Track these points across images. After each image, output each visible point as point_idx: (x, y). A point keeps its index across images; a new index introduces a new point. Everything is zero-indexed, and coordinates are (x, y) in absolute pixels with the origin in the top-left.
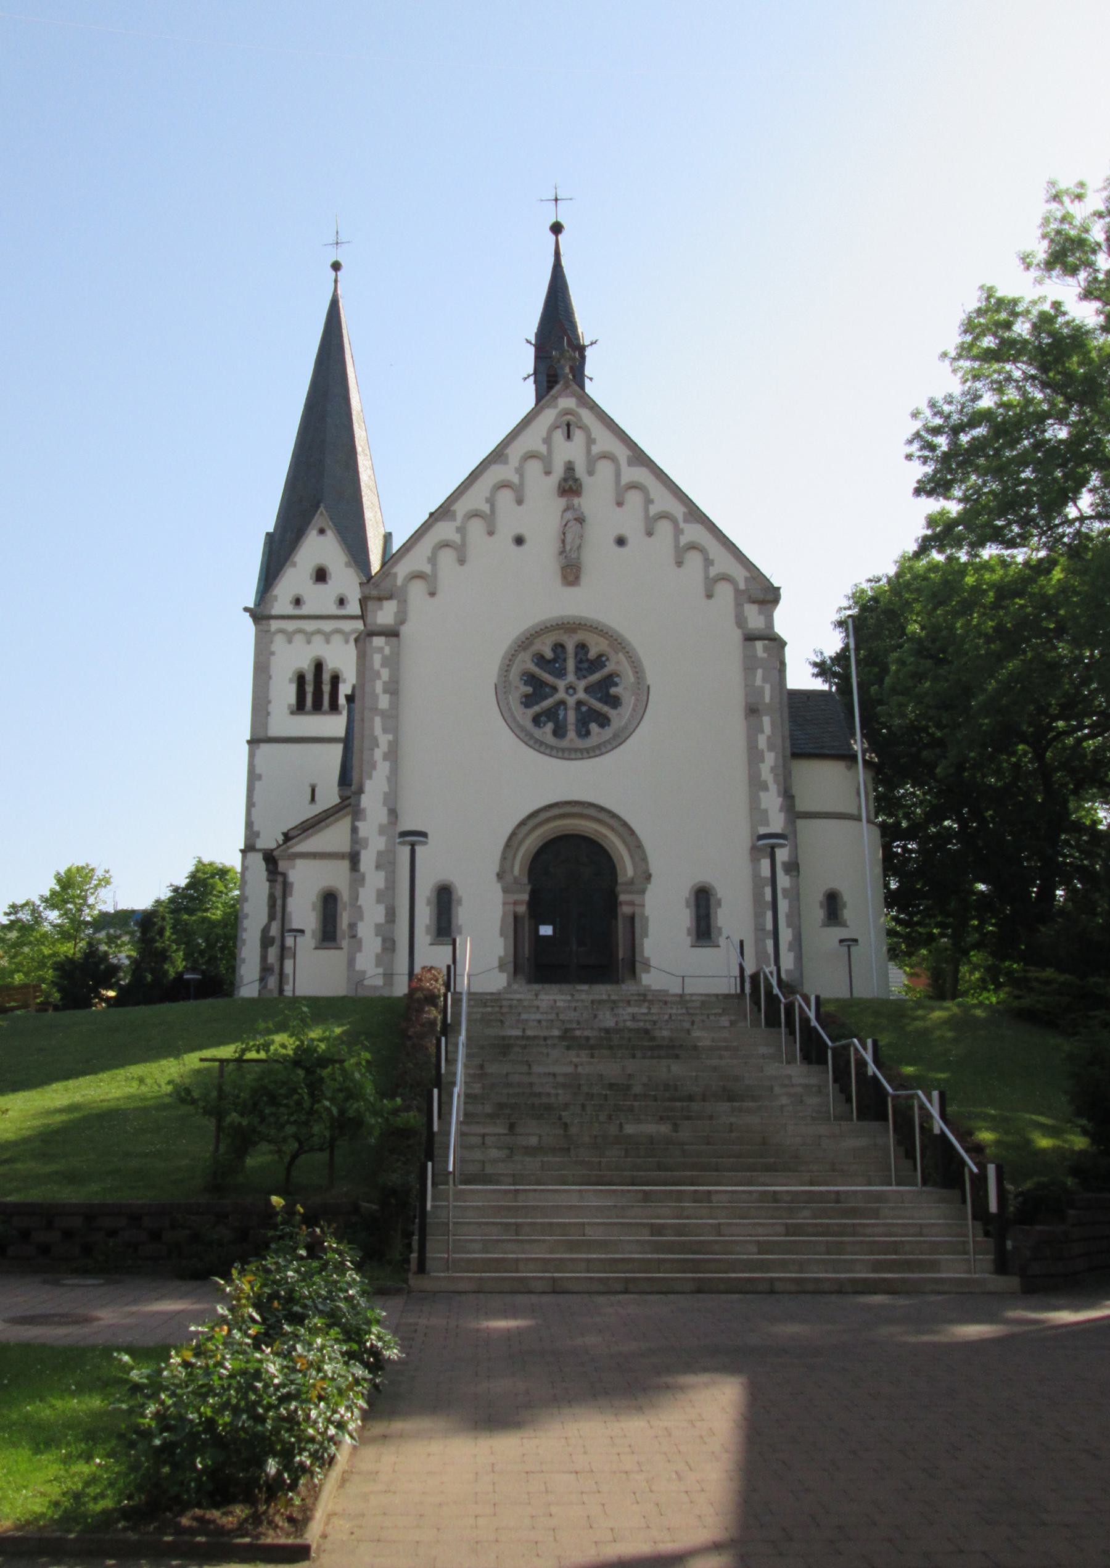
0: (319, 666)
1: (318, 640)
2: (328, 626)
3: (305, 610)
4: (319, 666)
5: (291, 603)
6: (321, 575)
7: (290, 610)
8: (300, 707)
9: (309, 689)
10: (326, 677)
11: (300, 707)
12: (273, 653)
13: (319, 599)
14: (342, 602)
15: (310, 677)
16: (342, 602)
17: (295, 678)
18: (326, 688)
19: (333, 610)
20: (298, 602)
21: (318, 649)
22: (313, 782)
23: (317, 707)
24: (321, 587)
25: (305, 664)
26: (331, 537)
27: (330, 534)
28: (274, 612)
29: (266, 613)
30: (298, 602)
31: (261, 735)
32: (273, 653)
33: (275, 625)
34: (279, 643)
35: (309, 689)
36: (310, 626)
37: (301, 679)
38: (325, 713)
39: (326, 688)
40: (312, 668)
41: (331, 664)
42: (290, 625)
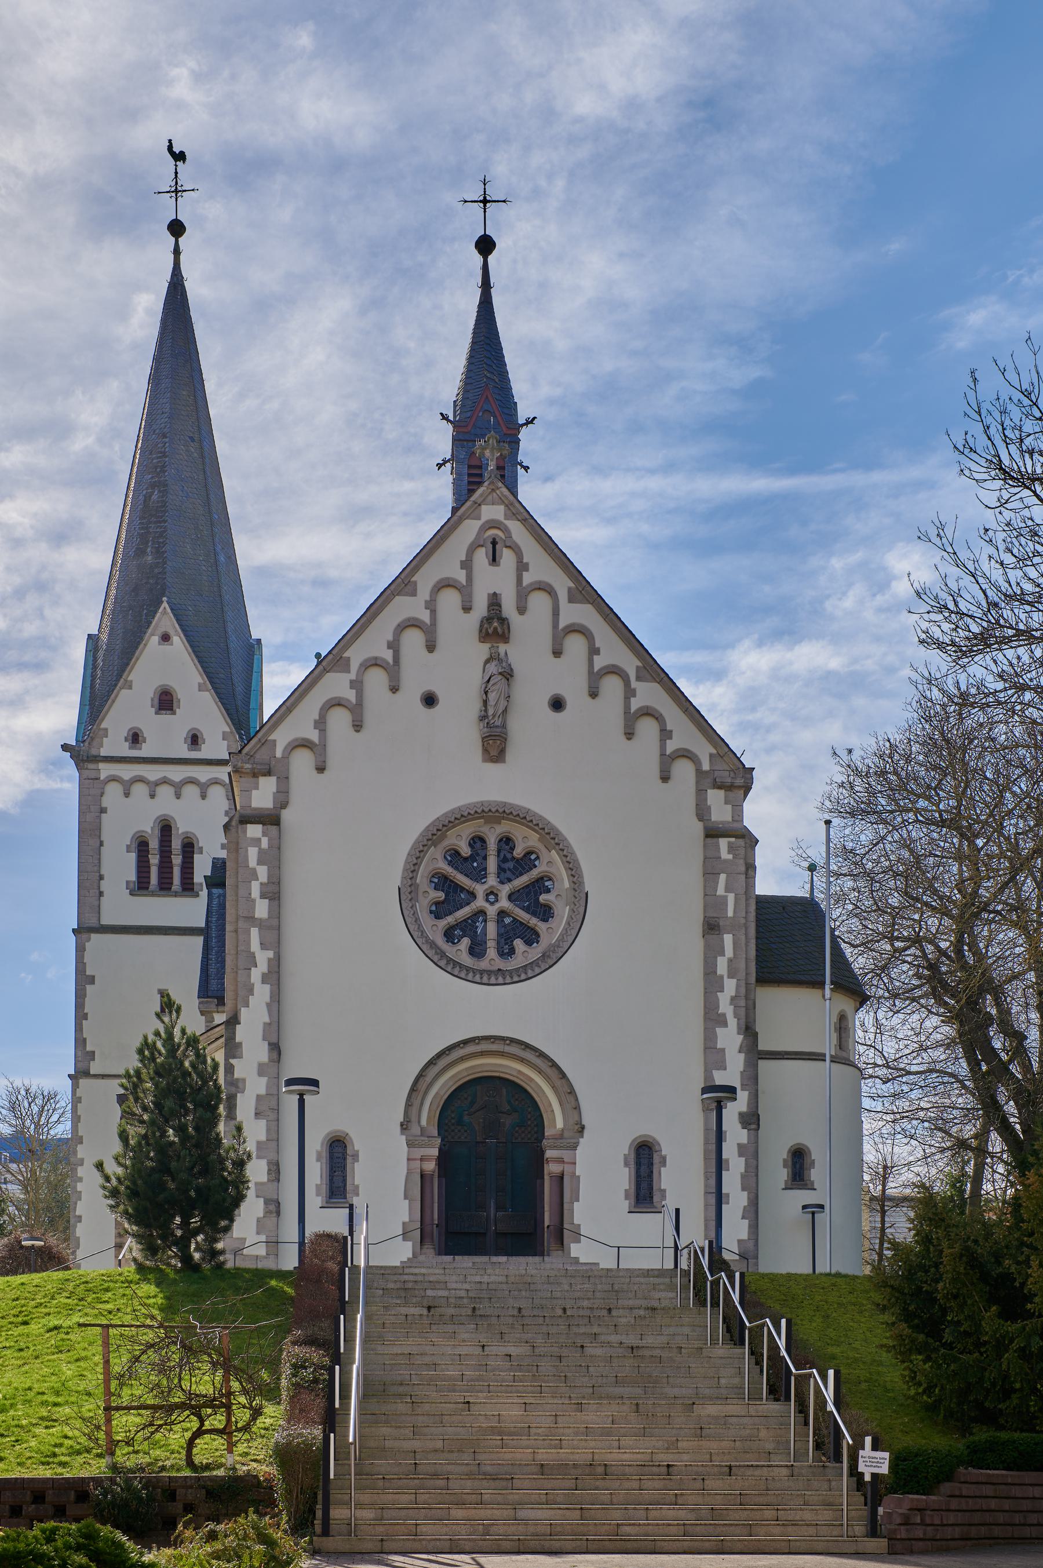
0: (166, 829)
1: (165, 792)
4: (166, 829)
5: (126, 740)
6: (166, 702)
7: (125, 751)
8: (141, 886)
9: (154, 860)
10: (176, 845)
11: (141, 886)
12: (103, 810)
14: (195, 740)
15: (154, 844)
16: (195, 740)
17: (134, 846)
18: (177, 860)
19: (184, 752)
20: (135, 738)
21: (166, 804)
23: (165, 887)
24: (166, 718)
25: (148, 826)
28: (103, 752)
29: (94, 752)
30: (135, 738)
31: (92, 922)
32: (103, 810)
33: (106, 770)
34: (113, 794)
35: (154, 860)
36: (153, 773)
37: (142, 846)
38: (176, 895)
39: (177, 860)
40: (157, 832)
41: (182, 827)
42: (127, 772)
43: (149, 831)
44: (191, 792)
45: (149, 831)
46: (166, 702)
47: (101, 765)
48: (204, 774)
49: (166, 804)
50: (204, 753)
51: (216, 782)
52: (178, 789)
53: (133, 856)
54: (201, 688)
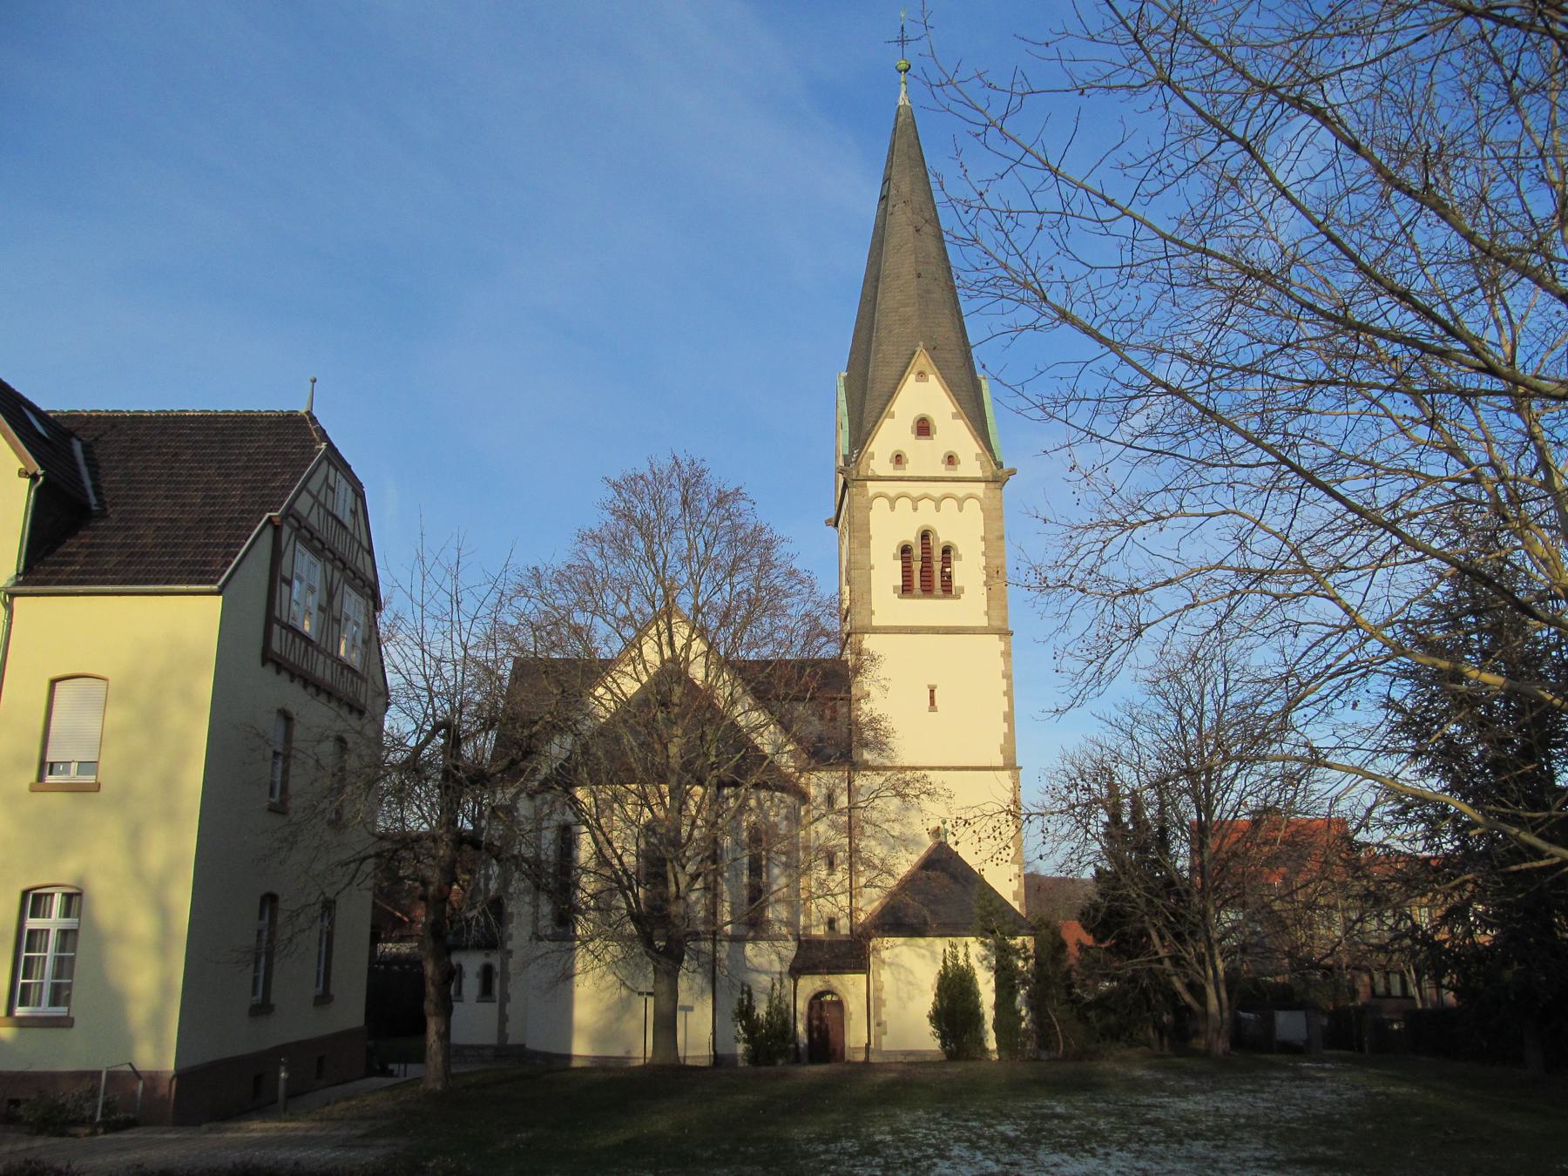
2: (937, 489)
4: (925, 535)
6: (923, 428)
8: (906, 589)
10: (937, 553)
11: (906, 589)
13: (925, 457)
14: (951, 460)
15: (917, 552)
16: (951, 460)
18: (937, 566)
19: (942, 471)
20: (898, 459)
22: (932, 683)
23: (927, 590)
24: (924, 442)
25: (912, 537)
26: (934, 384)
27: (932, 378)
30: (898, 459)
35: (917, 566)
37: (905, 550)
38: (938, 597)
39: (937, 566)
41: (943, 537)
42: (892, 488)
44: (949, 504)
46: (923, 428)
47: (869, 483)
48: (960, 489)
49: (926, 516)
50: (961, 471)
52: (938, 502)
53: (900, 562)
54: (955, 416)
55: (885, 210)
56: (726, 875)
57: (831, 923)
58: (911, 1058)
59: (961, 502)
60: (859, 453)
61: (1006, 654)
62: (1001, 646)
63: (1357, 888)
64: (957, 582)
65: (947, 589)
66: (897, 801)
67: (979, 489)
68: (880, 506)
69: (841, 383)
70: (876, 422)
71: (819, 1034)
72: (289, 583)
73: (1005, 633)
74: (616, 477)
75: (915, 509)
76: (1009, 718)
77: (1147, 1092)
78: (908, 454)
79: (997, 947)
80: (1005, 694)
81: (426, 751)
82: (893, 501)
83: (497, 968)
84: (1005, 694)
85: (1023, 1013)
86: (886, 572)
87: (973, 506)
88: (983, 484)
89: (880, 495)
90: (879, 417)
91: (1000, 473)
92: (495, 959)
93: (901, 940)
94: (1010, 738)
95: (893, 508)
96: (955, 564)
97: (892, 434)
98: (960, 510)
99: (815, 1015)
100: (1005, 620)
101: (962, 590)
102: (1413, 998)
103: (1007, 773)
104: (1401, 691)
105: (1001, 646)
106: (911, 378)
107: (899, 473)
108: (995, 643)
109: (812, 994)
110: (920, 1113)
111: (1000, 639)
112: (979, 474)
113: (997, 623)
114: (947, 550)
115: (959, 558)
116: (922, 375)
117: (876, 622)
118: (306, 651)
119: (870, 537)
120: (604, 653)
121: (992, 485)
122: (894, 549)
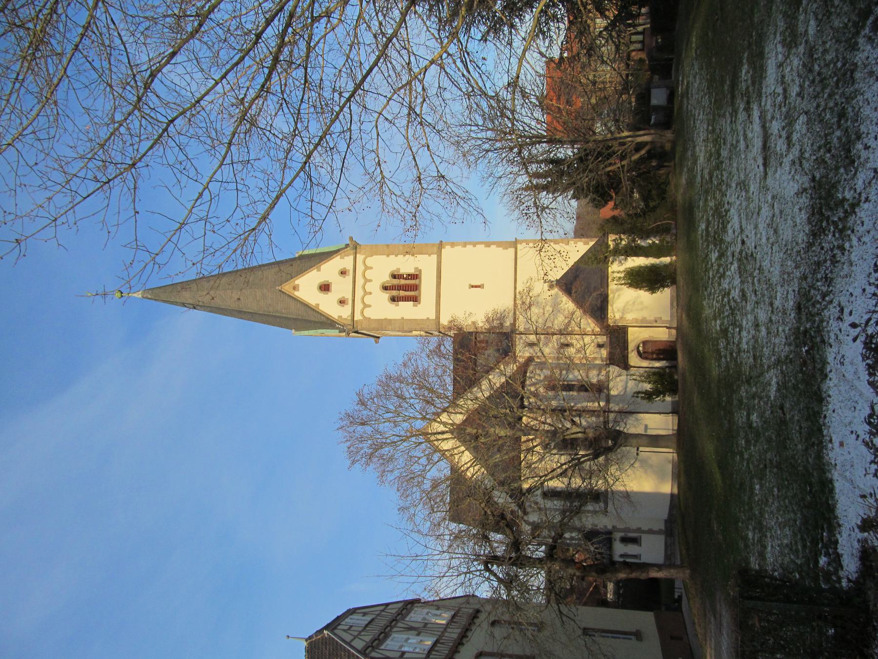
1: (368, 287)
3: (349, 297)
4: (385, 288)
6: (325, 288)
8: (415, 299)
10: (396, 282)
11: (415, 299)
13: (341, 287)
14: (343, 273)
15: (395, 293)
16: (343, 273)
18: (403, 282)
19: (349, 278)
20: (342, 302)
22: (468, 286)
23: (416, 288)
25: (386, 296)
29: (350, 322)
30: (342, 302)
33: (358, 317)
35: (402, 293)
36: (359, 293)
37: (393, 299)
38: (420, 282)
39: (403, 282)
41: (386, 278)
42: (359, 306)
43: (388, 295)
44: (368, 274)
45: (388, 295)
46: (325, 288)
47: (355, 319)
48: (360, 268)
49: (375, 287)
50: (350, 268)
51: (364, 262)
52: (367, 281)
53: (400, 303)
54: (319, 270)
55: (201, 306)
56: (572, 404)
57: (600, 346)
58: (675, 304)
59: (367, 268)
60: (338, 324)
61: (453, 245)
62: (448, 248)
63: (584, 59)
64: (412, 271)
65: (415, 276)
66: (533, 309)
67: (360, 257)
68: (368, 313)
69: (298, 333)
70: (321, 314)
71: (661, 354)
72: (403, 653)
73: (441, 245)
74: (349, 462)
75: (370, 293)
76: (488, 244)
77: (695, 177)
78: (340, 296)
79: (614, 255)
80: (475, 246)
81: (501, 576)
82: (366, 306)
83: (622, 534)
84: (475, 246)
85: (650, 242)
86: (405, 310)
87: (370, 261)
88: (358, 255)
89: (362, 313)
90: (318, 312)
91: (352, 246)
92: (618, 535)
93: (610, 307)
94: (499, 244)
95: (369, 306)
96: (402, 271)
97: (328, 305)
98: (371, 268)
99: (650, 356)
100: (433, 245)
101: (416, 269)
102: (644, 29)
103: (519, 246)
104: (477, 32)
105: (448, 248)
106: (297, 294)
107: (350, 302)
108: (446, 251)
109: (639, 358)
110: (705, 303)
111: (444, 248)
112: (351, 257)
113: (435, 250)
114: (394, 276)
115: (398, 269)
116: (295, 288)
117: (433, 316)
118: (442, 643)
119: (385, 319)
120: (448, 472)
121: (358, 250)
122: (392, 306)
